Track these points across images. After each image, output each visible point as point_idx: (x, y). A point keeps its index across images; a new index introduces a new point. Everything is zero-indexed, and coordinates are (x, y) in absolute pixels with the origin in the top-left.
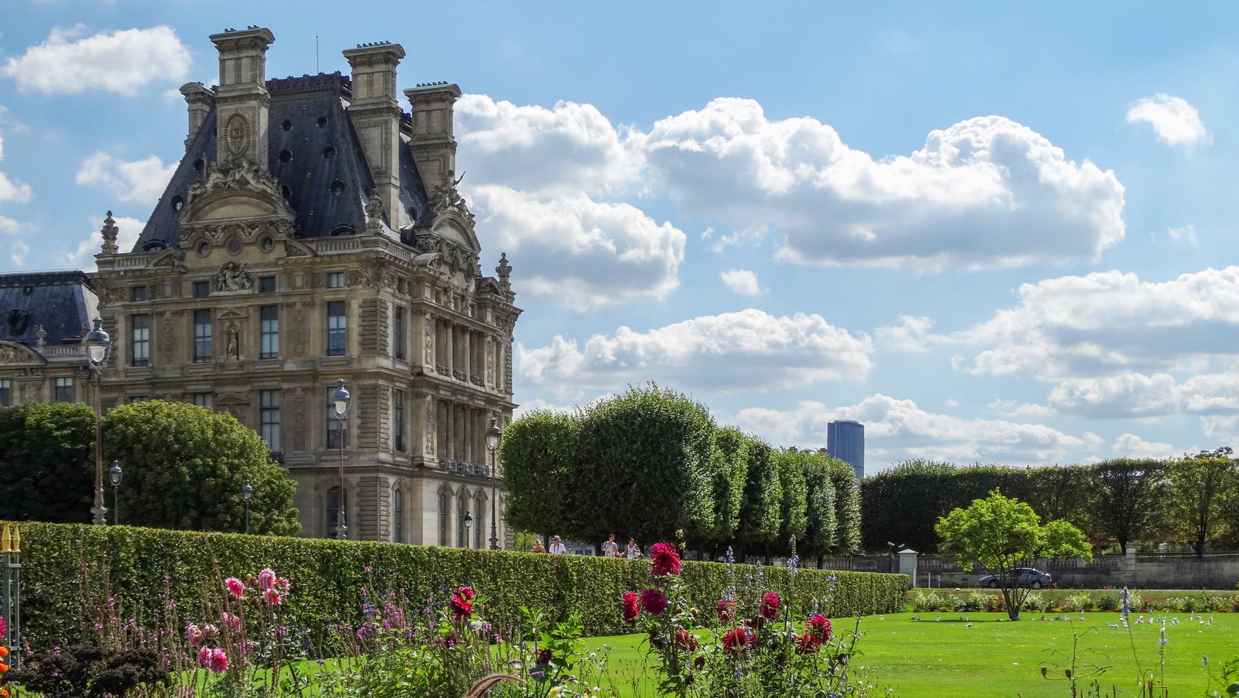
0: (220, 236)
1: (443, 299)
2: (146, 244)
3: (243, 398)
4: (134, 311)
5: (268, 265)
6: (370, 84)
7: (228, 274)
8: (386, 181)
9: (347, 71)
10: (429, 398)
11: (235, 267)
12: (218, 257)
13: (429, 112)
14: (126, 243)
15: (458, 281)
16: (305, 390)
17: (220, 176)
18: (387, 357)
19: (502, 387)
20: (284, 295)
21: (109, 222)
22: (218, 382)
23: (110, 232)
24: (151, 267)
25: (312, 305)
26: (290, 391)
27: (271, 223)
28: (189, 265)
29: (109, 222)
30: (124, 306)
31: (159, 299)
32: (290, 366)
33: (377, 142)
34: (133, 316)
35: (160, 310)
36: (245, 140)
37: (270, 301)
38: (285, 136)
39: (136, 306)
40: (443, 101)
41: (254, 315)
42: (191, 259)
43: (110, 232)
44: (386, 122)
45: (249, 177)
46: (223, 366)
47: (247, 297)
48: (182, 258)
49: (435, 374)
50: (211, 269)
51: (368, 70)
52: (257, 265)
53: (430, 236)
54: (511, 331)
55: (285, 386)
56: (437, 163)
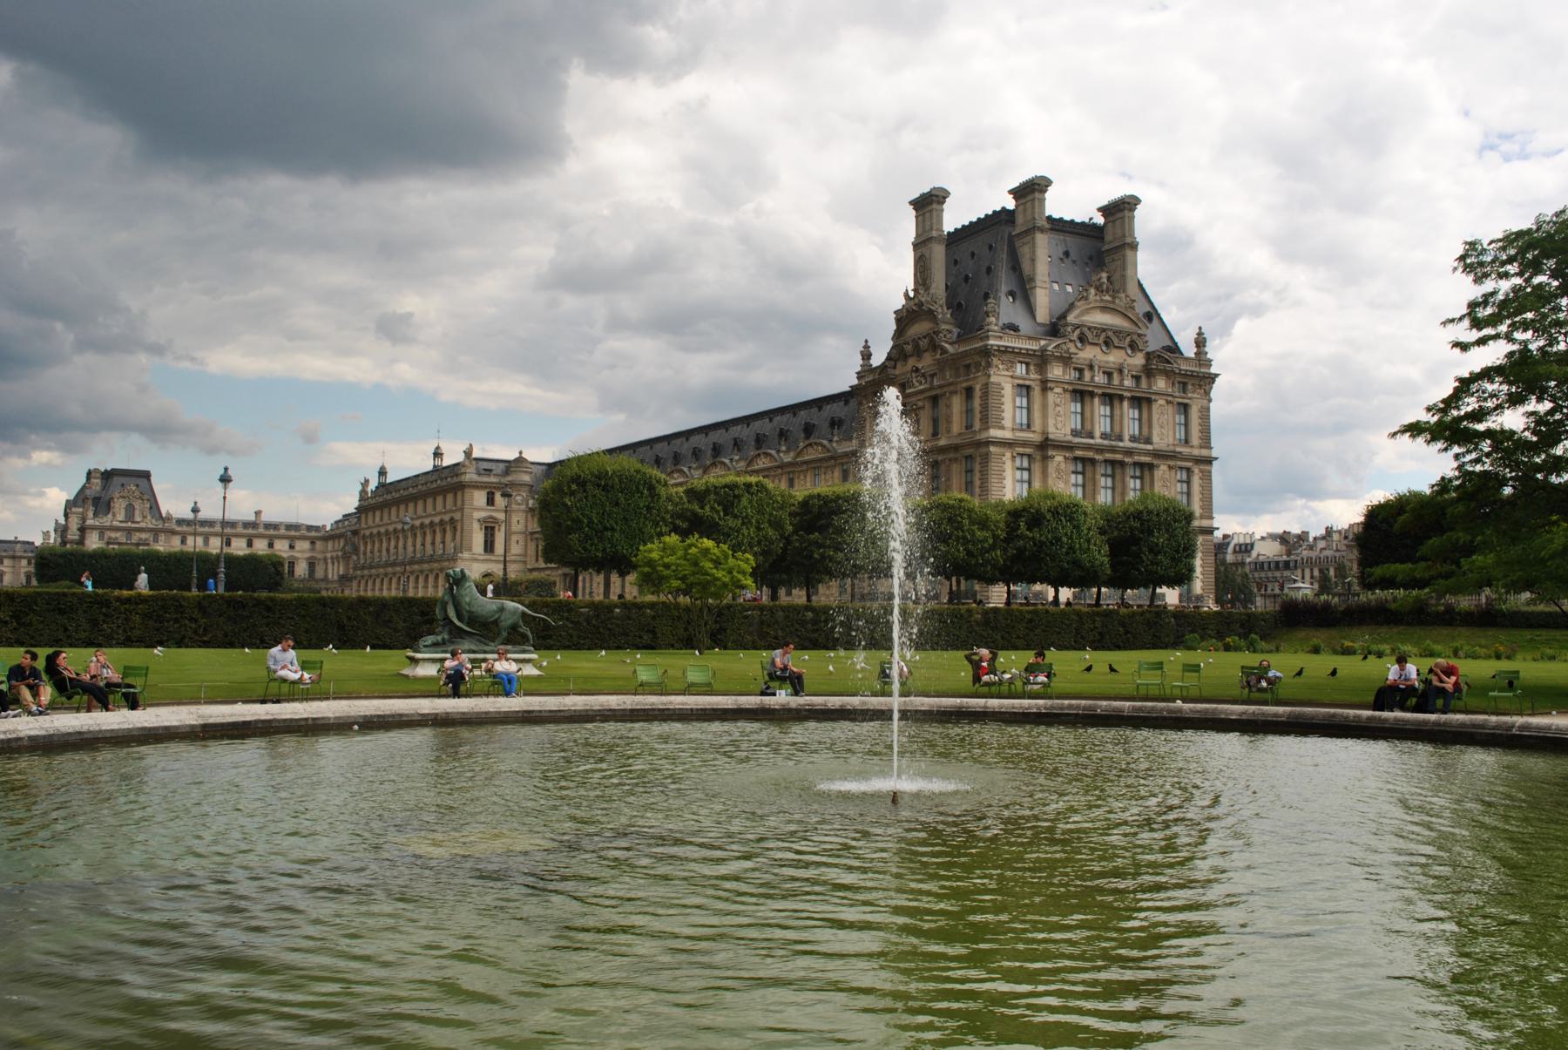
9: (1010, 204)
10: (1059, 458)
11: (917, 370)
12: (911, 362)
14: (878, 359)
15: (1114, 358)
18: (1003, 428)
19: (1195, 441)
20: (941, 387)
21: (867, 347)
25: (955, 392)
29: (867, 347)
32: (942, 442)
37: (933, 393)
41: (928, 405)
47: (922, 392)
49: (1070, 438)
53: (1067, 325)
54: (1207, 393)
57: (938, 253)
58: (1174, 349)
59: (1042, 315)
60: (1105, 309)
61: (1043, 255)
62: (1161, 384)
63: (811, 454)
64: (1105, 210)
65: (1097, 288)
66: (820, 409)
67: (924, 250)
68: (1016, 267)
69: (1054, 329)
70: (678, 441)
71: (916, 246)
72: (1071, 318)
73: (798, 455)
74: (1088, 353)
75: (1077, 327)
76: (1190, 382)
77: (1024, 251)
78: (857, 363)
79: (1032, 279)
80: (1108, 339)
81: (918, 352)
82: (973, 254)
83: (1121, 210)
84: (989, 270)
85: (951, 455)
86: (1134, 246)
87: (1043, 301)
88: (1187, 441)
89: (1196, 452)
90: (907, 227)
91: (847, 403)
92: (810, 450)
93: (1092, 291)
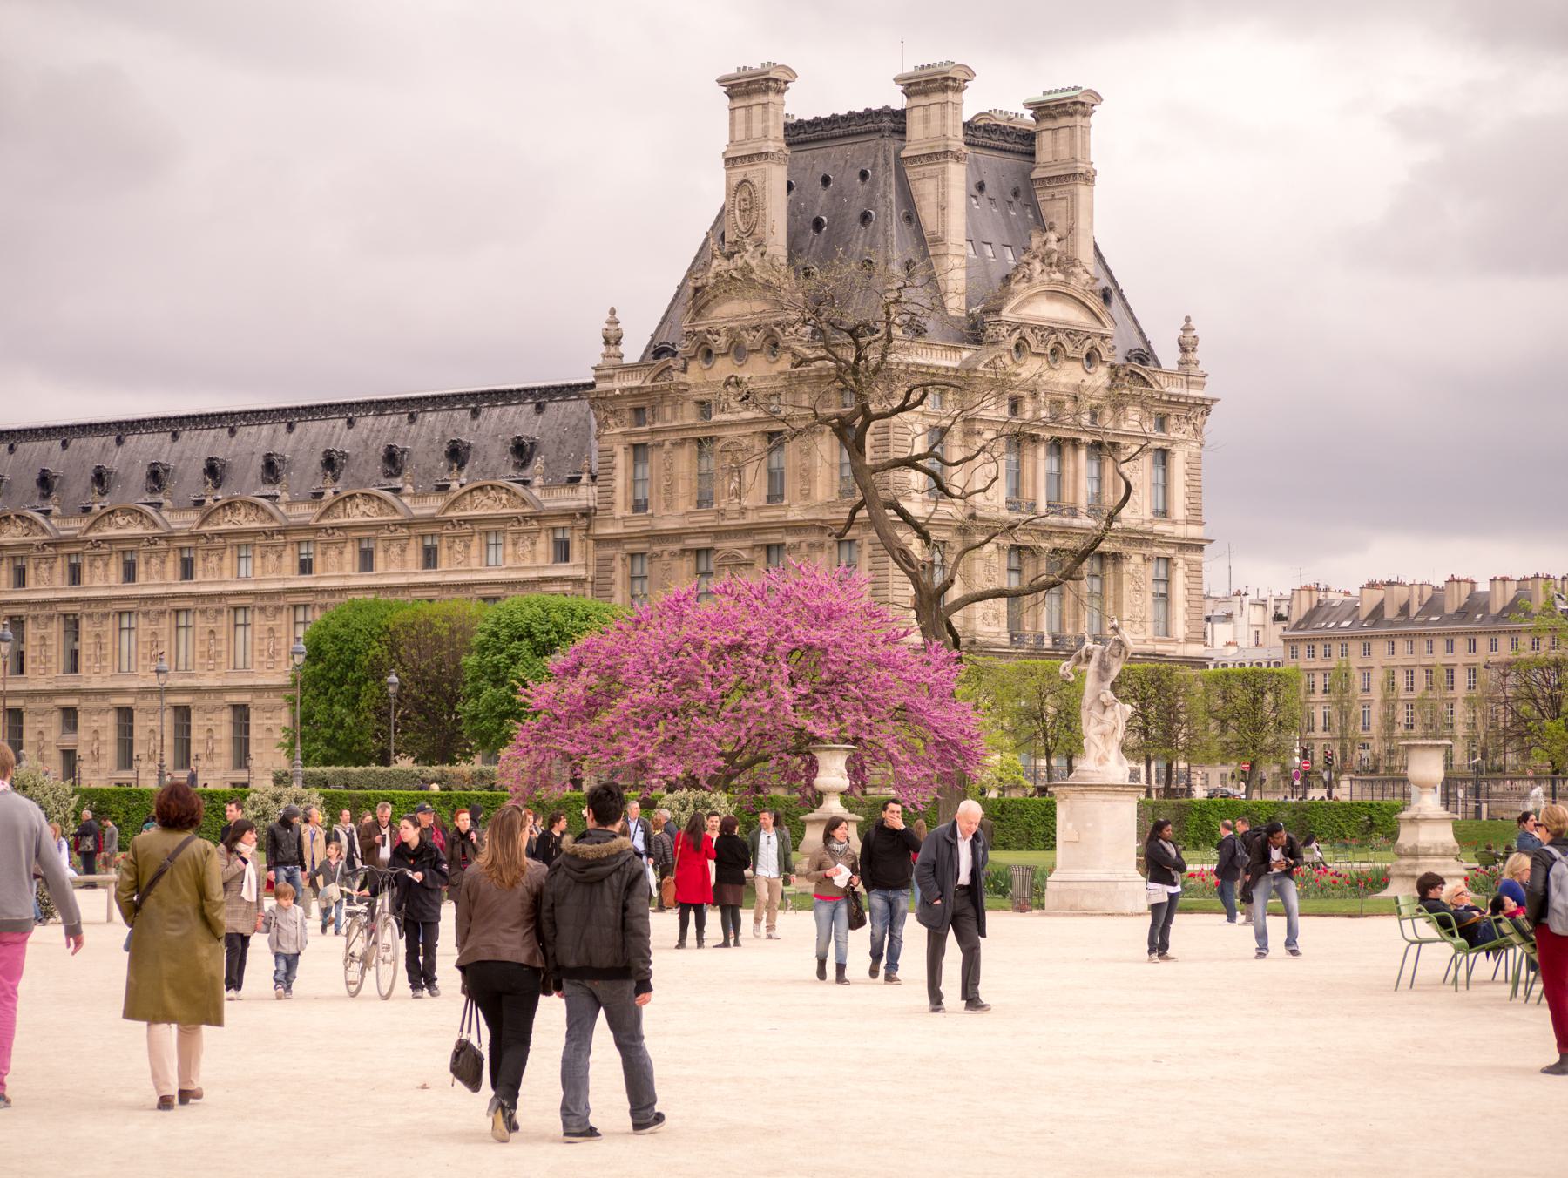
0: (722, 340)
1: (1028, 407)
2: (659, 349)
3: (745, 555)
4: (635, 440)
5: (774, 378)
6: (926, 120)
7: (730, 389)
8: (942, 250)
9: (898, 101)
12: (723, 367)
13: (1055, 130)
14: (633, 349)
15: (1069, 375)
16: (811, 546)
17: (725, 263)
19: (1179, 510)
22: (719, 534)
23: (612, 340)
24: (648, 383)
26: (796, 547)
27: (777, 324)
28: (689, 378)
30: (624, 434)
31: (658, 425)
32: (795, 515)
33: (933, 199)
34: (636, 447)
35: (659, 438)
36: (754, 213)
38: (823, 195)
39: (637, 434)
40: (1072, 115)
41: (760, 445)
42: (695, 374)
43: (612, 340)
44: (943, 171)
45: (753, 263)
46: (721, 513)
48: (685, 370)
49: (1004, 514)
50: (713, 384)
51: (923, 101)
52: (764, 378)
53: (1000, 323)
55: (789, 540)
56: (1064, 203)
57: (774, 179)
58: (1144, 356)
59: (956, 305)
60: (1053, 295)
61: (951, 198)
62: (1133, 420)
63: (484, 507)
64: (1043, 110)
65: (1043, 261)
66: (475, 413)
67: (739, 173)
68: (911, 217)
69: (974, 332)
70: (96, 442)
71: (730, 161)
72: (1006, 314)
73: (453, 504)
74: (1030, 368)
75: (1017, 327)
76: (1174, 412)
77: (925, 191)
78: (596, 352)
79: (938, 241)
80: (1058, 344)
81: (738, 351)
82: (826, 181)
83: (1065, 110)
84: (865, 218)
85: (814, 538)
86: (1089, 178)
87: (956, 277)
88: (1164, 514)
89: (1181, 531)
90: (714, 123)
91: (540, 408)
92: (478, 495)
93: (1037, 266)
